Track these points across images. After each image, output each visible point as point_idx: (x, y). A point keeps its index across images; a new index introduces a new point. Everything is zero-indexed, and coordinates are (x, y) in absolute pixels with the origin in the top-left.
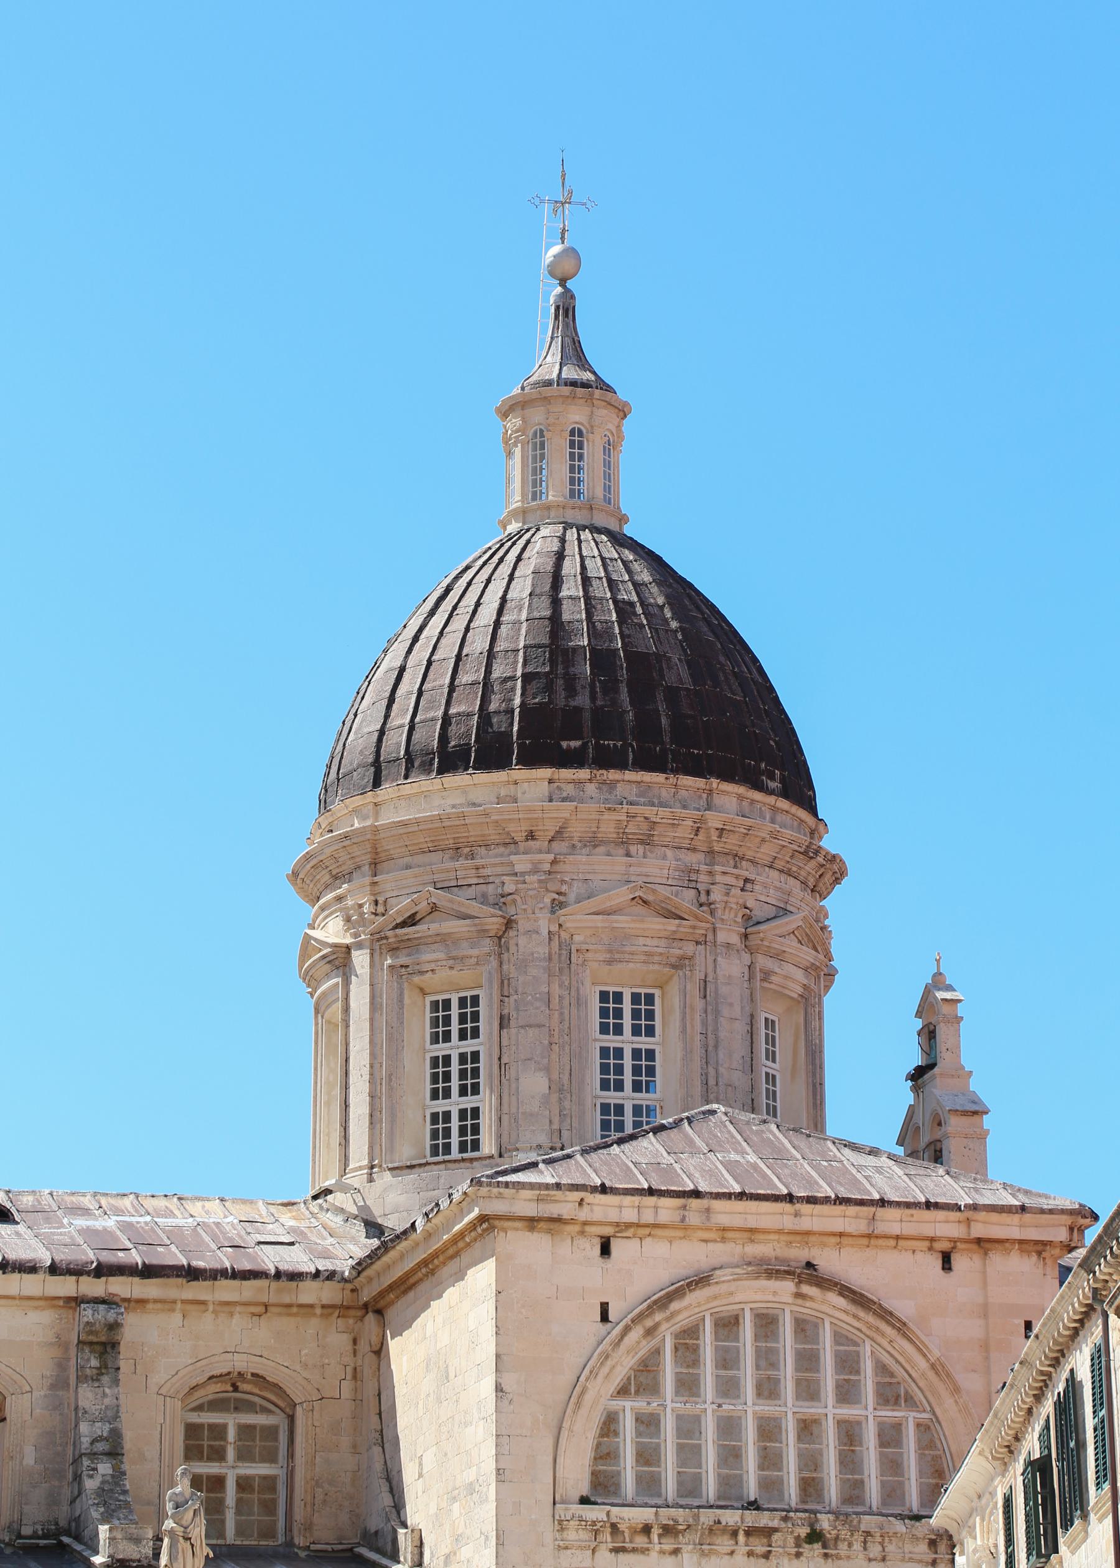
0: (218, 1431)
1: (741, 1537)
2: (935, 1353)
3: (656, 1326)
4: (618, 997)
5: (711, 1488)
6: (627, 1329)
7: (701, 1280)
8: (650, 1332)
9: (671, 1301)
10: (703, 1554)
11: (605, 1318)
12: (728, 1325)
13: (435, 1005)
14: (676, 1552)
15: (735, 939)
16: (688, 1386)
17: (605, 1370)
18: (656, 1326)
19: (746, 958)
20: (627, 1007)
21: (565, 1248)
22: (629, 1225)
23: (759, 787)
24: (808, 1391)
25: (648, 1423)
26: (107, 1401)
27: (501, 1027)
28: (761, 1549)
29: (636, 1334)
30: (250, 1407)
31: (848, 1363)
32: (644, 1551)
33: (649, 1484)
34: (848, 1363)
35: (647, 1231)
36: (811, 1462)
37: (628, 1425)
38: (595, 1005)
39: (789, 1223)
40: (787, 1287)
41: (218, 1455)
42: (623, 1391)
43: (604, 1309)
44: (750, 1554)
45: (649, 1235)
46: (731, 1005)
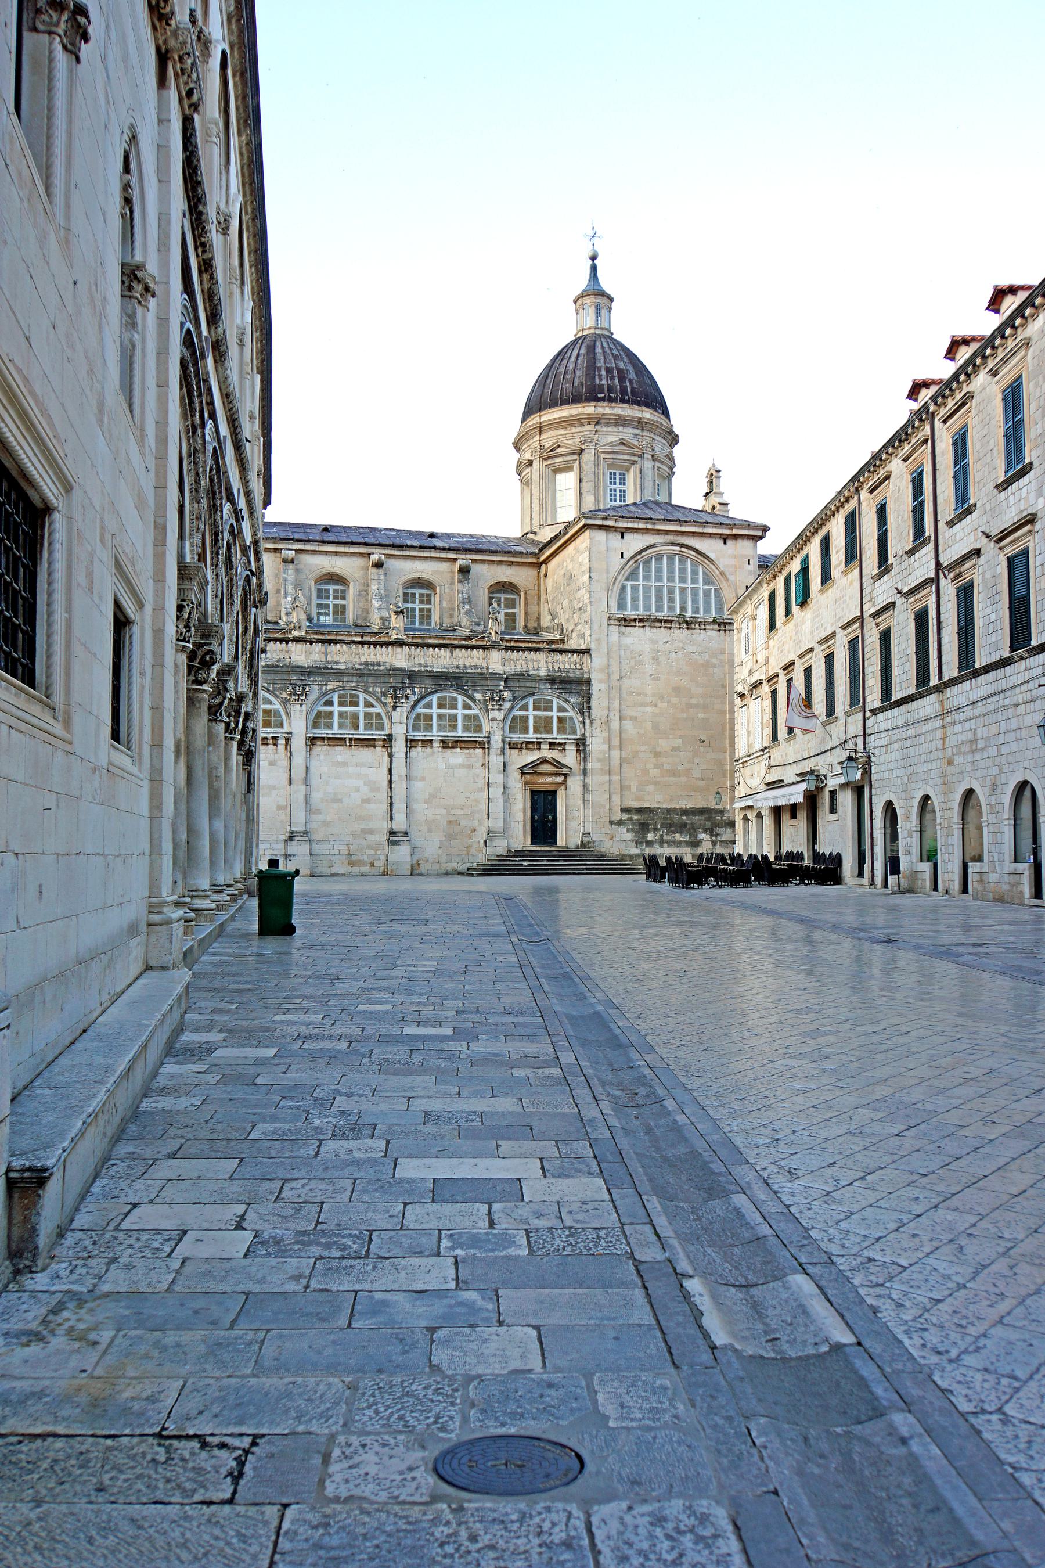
2: (722, 568)
6: (629, 560)
7: (652, 546)
16: (647, 578)
21: (610, 536)
24: (683, 580)
25: (635, 588)
31: (694, 572)
33: (635, 607)
34: (694, 572)
36: (683, 601)
38: (608, 476)
39: (678, 528)
40: (678, 548)
42: (627, 579)
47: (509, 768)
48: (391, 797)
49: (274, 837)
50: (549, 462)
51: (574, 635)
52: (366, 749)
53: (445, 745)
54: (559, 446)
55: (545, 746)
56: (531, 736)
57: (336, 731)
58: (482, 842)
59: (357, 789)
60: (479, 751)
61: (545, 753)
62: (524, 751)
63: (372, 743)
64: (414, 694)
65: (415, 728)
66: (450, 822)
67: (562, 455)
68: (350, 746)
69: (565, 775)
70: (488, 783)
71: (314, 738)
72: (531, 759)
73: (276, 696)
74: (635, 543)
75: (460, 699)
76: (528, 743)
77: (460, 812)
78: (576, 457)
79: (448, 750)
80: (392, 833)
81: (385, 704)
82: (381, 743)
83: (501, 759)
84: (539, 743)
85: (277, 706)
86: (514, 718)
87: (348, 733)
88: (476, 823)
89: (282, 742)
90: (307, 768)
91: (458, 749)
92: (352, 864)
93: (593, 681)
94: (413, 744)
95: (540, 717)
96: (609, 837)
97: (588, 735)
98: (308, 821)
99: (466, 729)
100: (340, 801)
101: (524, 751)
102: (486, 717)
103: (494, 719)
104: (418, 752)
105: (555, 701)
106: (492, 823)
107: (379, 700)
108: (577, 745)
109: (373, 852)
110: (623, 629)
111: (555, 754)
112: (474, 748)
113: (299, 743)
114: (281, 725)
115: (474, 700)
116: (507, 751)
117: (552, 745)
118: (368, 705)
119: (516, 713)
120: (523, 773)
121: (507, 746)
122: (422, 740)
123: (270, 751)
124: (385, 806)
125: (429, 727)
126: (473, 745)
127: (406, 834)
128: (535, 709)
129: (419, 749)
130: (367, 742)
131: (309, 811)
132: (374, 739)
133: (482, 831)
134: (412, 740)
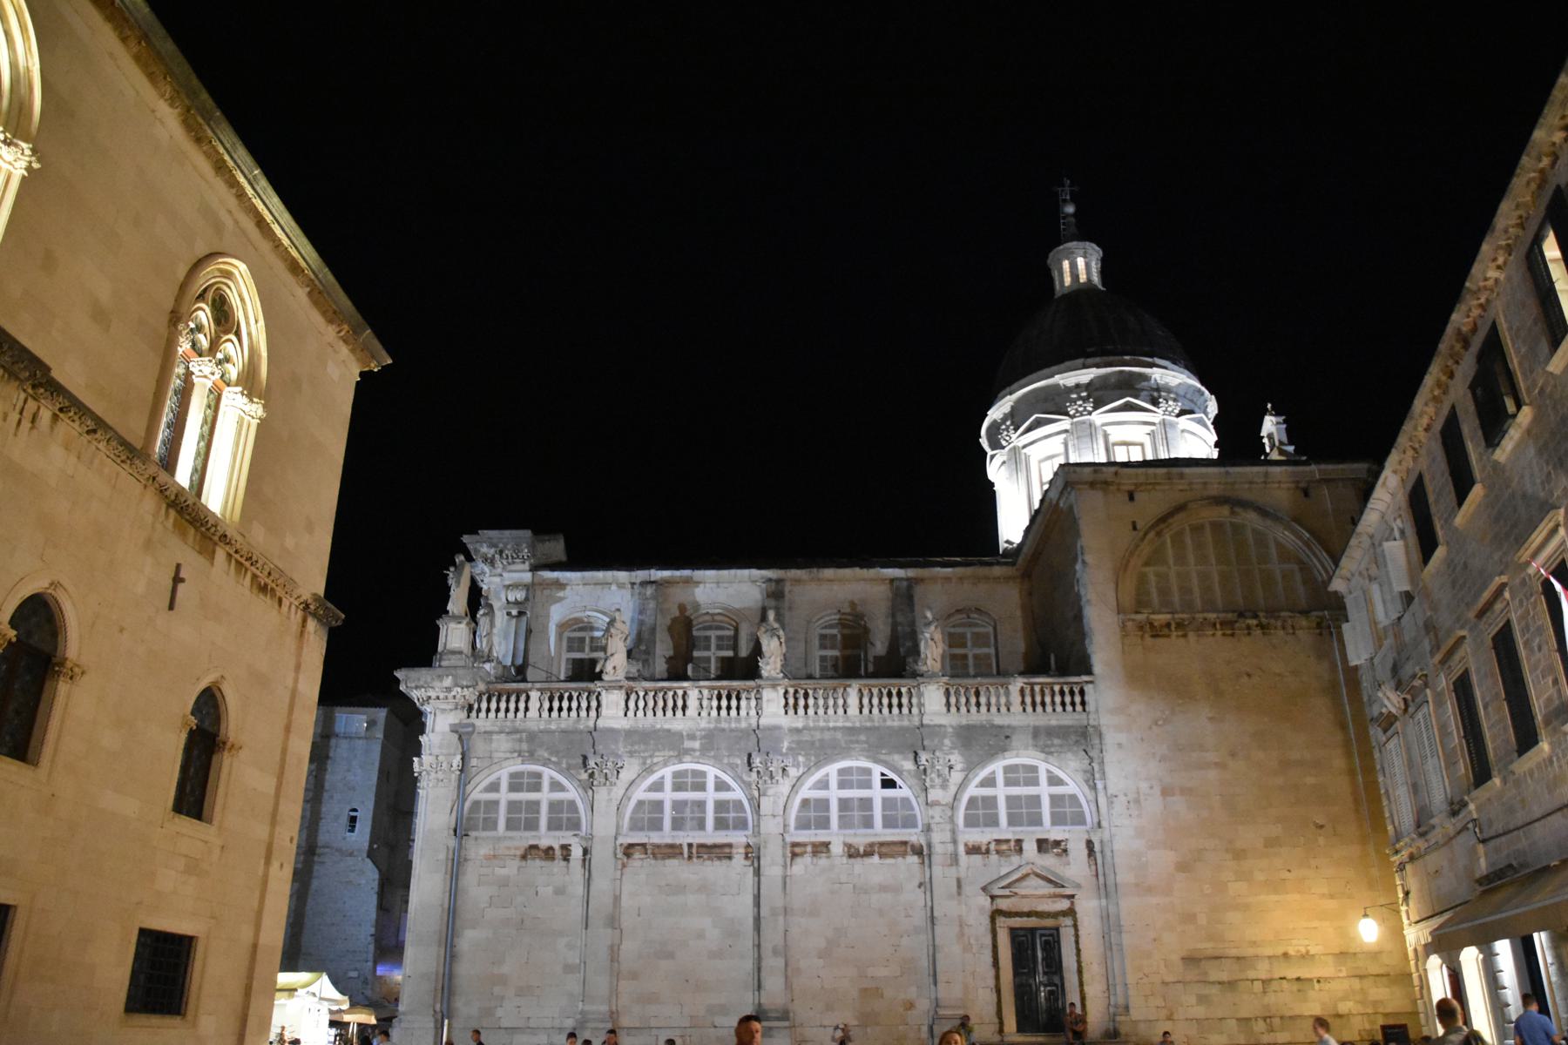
0: (963, 636)
1: (1218, 626)
5: (1198, 603)
8: (1159, 534)
10: (1199, 636)
11: (1135, 528)
12: (1197, 529)
14: (1185, 636)
16: (1181, 559)
17: (1137, 553)
18: (1161, 530)
22: (1141, 484)
28: (1229, 632)
29: (1152, 535)
30: (976, 625)
32: (1168, 636)
35: (1151, 487)
37: (1152, 579)
41: (964, 645)
44: (1224, 635)
47: (967, 889)
48: (759, 946)
49: (557, 1023)
52: (717, 863)
53: (852, 853)
55: (1030, 847)
56: (1005, 831)
57: (666, 836)
58: (925, 1029)
59: (700, 935)
60: (915, 859)
62: (994, 857)
63: (727, 850)
64: (797, 766)
65: (803, 824)
66: (865, 992)
68: (690, 857)
69: (1073, 896)
70: (932, 918)
71: (631, 846)
73: (570, 777)
75: (877, 770)
76: (998, 842)
77: (882, 972)
79: (859, 859)
81: (746, 786)
82: (742, 850)
83: (952, 872)
84: (1019, 842)
85: (572, 793)
87: (685, 838)
88: (912, 993)
89: (577, 852)
90: (617, 899)
91: (876, 858)
93: (1104, 730)
94: (797, 850)
95: (1018, 798)
96: (1163, 1013)
97: (1104, 824)
98: (614, 992)
99: (889, 822)
100: (671, 956)
101: (994, 857)
102: (922, 799)
103: (936, 804)
104: (800, 867)
105: (1043, 768)
106: (943, 992)
107: (737, 778)
108: (1090, 844)
110: (1149, 640)
112: (904, 855)
113: (603, 855)
114: (575, 825)
115: (899, 773)
116: (964, 858)
118: (721, 786)
119: (973, 790)
120: (993, 898)
121: (961, 849)
122: (814, 845)
124: (749, 965)
125: (824, 823)
126: (903, 848)
127: (785, 1015)
128: (1008, 783)
129: (807, 859)
130: (720, 852)
131: (616, 975)
132: (730, 846)
133: (924, 1005)
134: (794, 845)
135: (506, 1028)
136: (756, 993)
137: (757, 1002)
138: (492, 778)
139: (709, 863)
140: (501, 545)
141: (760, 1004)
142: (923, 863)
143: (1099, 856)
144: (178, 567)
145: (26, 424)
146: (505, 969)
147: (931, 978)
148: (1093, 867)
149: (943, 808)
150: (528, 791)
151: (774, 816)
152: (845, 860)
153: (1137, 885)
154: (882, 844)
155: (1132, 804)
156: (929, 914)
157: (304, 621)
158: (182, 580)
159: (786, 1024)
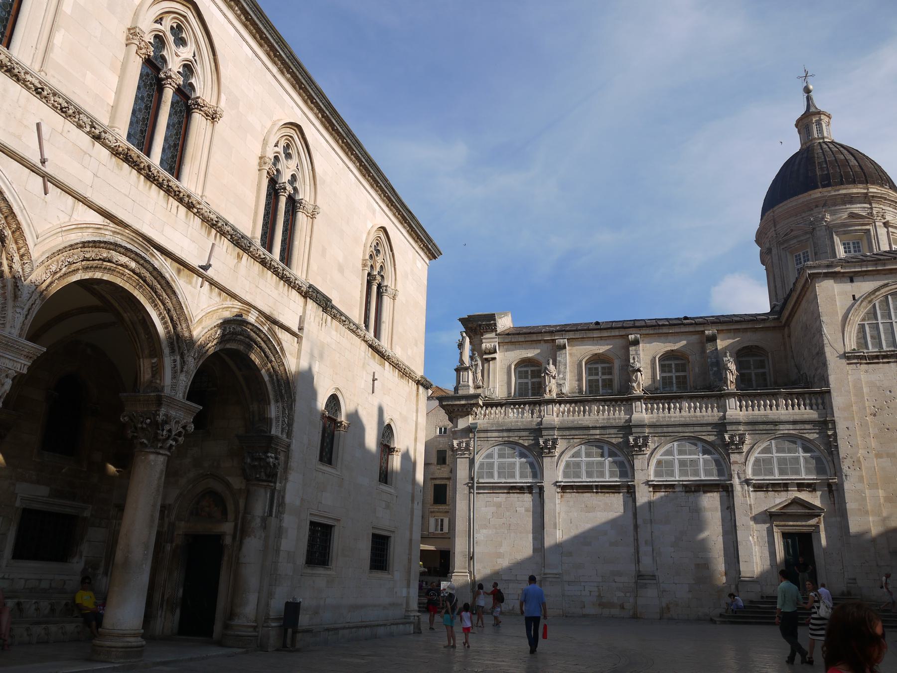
3: (872, 299)
4: (848, 244)
6: (862, 301)
9: (876, 292)
13: (796, 256)
14: (888, 362)
15: (881, 224)
18: (872, 299)
19: (886, 230)
20: (851, 246)
23: (883, 187)
26: (715, 354)
27: (815, 255)
29: (864, 304)
35: (865, 273)
42: (863, 320)
43: (854, 296)
45: (866, 275)
46: (883, 241)
48: (637, 540)
50: (786, 245)
51: (816, 380)
54: (792, 230)
56: (777, 476)
61: (794, 494)
66: (698, 566)
67: (795, 237)
72: (778, 501)
74: (864, 287)
78: (808, 236)
79: (692, 494)
80: (640, 576)
86: (757, 461)
92: (602, 605)
95: (785, 459)
109: (622, 594)
111: (805, 496)
117: (801, 486)
123: (526, 499)
124: (632, 550)
127: (653, 577)
135: (506, 580)
136: (637, 565)
137: (637, 569)
138: (489, 451)
139: (607, 495)
140: (480, 323)
141: (639, 571)
142: (729, 496)
143: (835, 493)
144: (374, 373)
145: (324, 324)
146: (502, 551)
147: (736, 559)
148: (832, 499)
149: (740, 465)
150: (508, 458)
151: (642, 470)
152: (683, 494)
153: (859, 510)
154: (705, 485)
155: (856, 463)
156: (733, 524)
157: (418, 389)
158: (376, 379)
159: (655, 582)
